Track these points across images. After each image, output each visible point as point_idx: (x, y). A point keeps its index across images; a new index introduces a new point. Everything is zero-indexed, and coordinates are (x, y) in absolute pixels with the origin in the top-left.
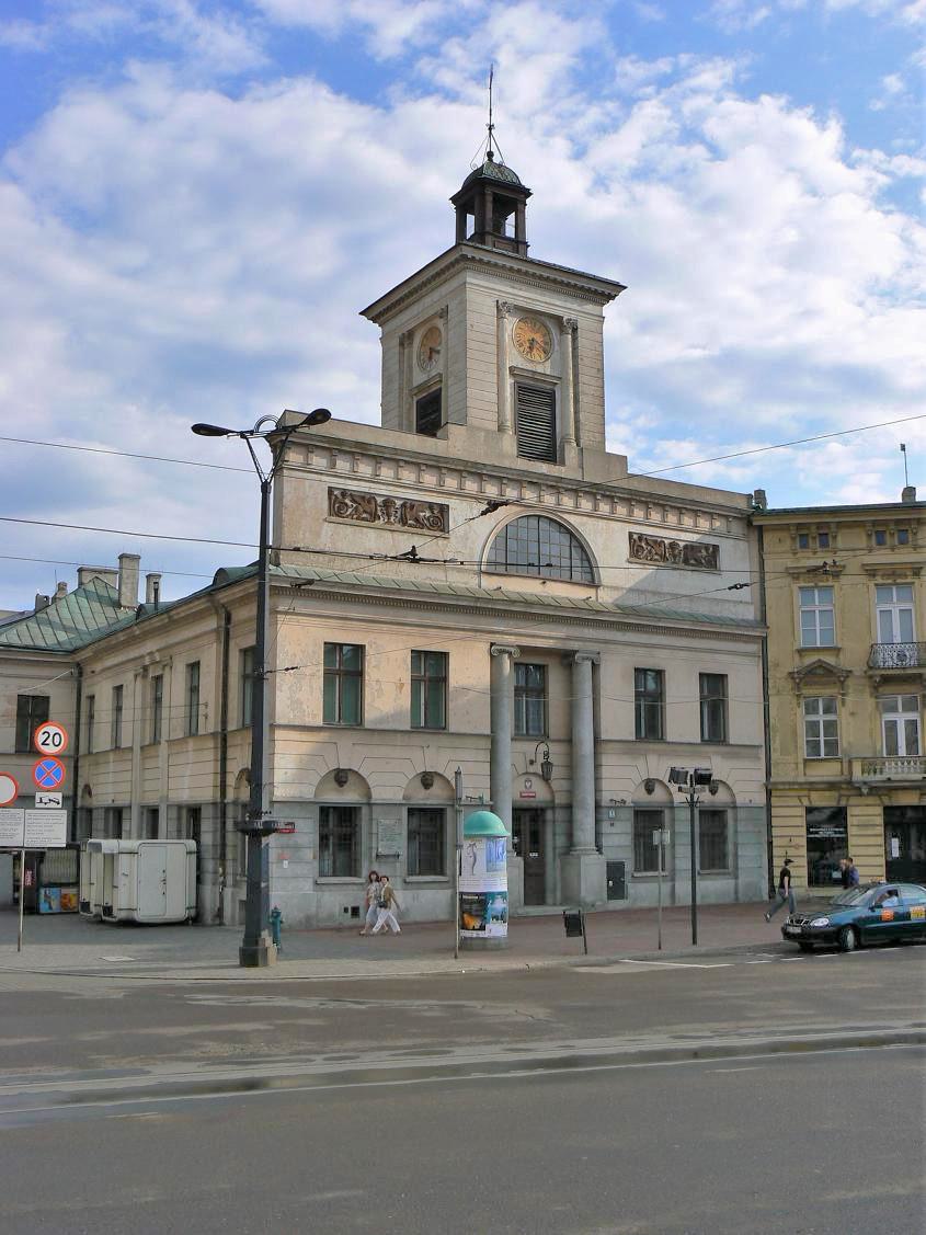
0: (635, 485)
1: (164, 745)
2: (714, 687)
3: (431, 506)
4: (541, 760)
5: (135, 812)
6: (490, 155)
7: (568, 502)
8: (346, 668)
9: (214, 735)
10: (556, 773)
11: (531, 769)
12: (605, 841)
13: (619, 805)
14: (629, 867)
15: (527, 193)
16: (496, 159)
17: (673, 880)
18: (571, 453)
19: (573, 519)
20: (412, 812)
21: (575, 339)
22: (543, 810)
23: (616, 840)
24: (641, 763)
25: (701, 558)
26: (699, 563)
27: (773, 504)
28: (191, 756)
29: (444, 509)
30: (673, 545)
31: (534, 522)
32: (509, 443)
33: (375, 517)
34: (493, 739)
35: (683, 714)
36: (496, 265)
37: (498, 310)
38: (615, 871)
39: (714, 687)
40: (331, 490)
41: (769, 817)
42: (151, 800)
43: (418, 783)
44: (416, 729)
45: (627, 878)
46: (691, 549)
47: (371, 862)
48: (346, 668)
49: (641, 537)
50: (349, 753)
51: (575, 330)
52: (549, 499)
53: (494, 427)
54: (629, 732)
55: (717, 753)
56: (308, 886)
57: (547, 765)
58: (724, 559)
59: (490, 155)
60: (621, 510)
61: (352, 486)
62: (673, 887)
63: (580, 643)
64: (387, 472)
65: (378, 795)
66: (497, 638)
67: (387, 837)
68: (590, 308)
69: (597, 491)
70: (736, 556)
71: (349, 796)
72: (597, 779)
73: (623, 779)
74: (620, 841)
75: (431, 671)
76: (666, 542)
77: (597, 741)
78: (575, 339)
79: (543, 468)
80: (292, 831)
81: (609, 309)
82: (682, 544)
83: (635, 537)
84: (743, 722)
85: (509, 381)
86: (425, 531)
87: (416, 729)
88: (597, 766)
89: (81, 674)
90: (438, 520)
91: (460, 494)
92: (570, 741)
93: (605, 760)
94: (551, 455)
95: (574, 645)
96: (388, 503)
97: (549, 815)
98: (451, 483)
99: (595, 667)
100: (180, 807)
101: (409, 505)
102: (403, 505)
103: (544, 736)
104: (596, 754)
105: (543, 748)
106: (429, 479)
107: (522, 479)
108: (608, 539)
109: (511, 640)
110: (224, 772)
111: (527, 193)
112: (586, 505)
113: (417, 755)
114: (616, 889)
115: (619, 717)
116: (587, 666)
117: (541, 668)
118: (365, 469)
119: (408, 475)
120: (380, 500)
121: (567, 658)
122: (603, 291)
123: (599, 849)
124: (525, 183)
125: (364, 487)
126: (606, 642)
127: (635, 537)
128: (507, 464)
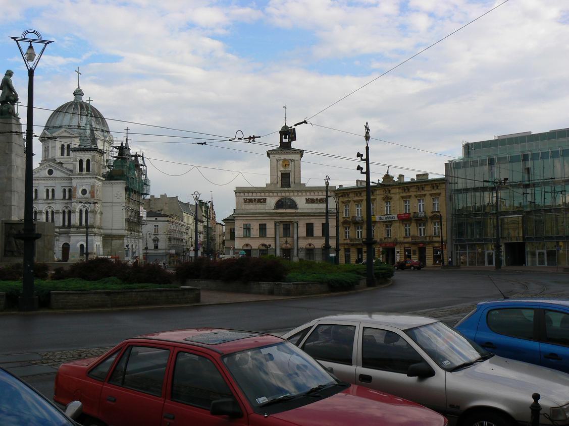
0: (307, 189)
3: (263, 199)
7: (292, 194)
8: (247, 229)
13: (302, 249)
18: (292, 185)
20: (260, 250)
23: (301, 255)
29: (266, 199)
32: (279, 185)
33: (252, 202)
34: (275, 238)
35: (318, 231)
40: (244, 199)
44: (260, 237)
48: (247, 229)
49: (309, 198)
50: (247, 241)
52: (287, 194)
54: (304, 234)
60: (304, 194)
64: (254, 194)
65: (253, 248)
66: (276, 220)
69: (298, 191)
71: (249, 248)
73: (303, 244)
75: (263, 228)
77: (298, 237)
79: (286, 189)
85: (280, 174)
87: (260, 237)
90: (265, 201)
91: (269, 196)
94: (289, 186)
96: (255, 200)
98: (267, 194)
106: (263, 194)
107: (281, 192)
112: (296, 194)
113: (260, 241)
115: (302, 232)
116: (295, 224)
117: (289, 224)
118: (250, 194)
119: (259, 194)
125: (250, 197)
126: (299, 219)
128: (278, 189)
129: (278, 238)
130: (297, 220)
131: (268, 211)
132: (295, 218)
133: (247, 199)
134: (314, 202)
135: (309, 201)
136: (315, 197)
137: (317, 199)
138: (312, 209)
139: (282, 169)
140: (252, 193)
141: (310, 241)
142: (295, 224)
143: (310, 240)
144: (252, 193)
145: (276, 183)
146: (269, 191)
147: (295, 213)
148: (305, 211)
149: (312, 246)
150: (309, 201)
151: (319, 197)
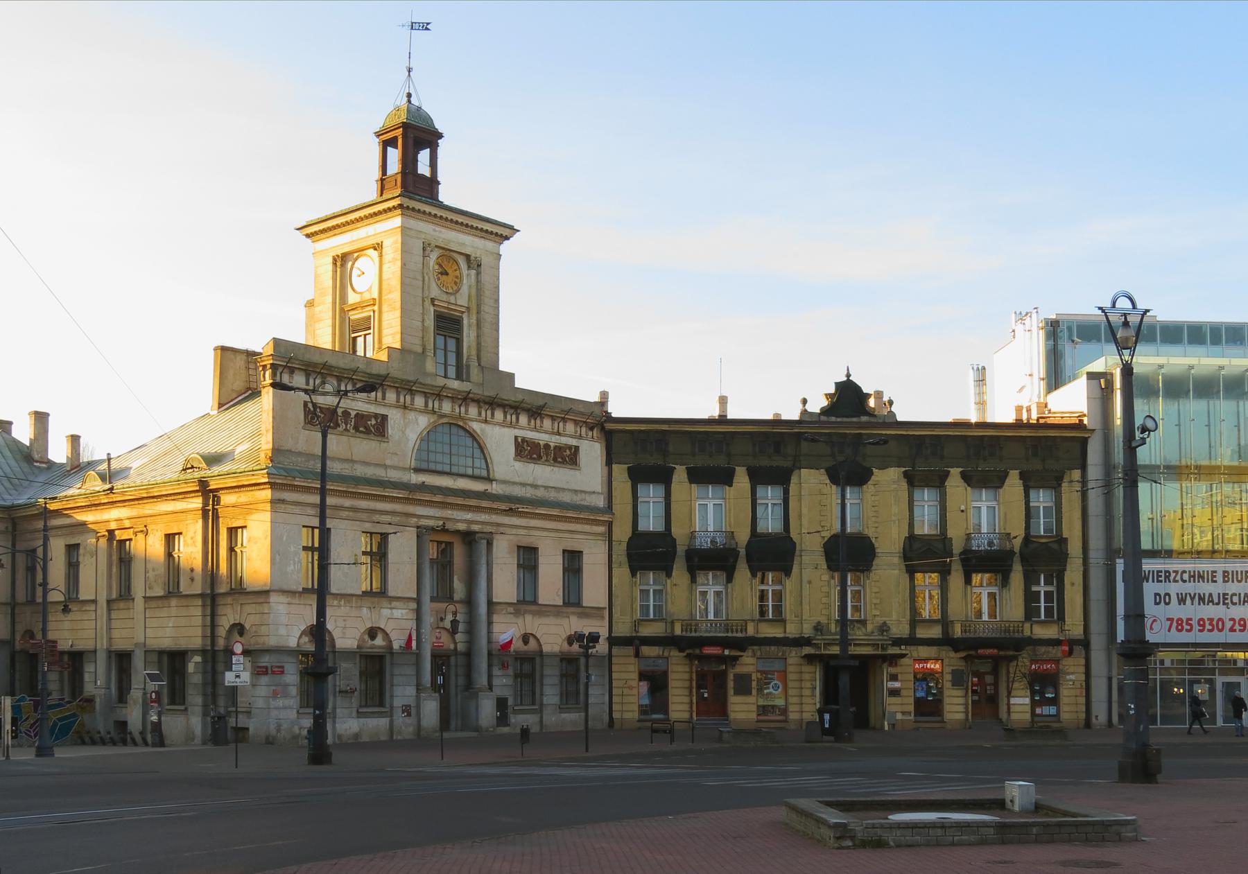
1: (139, 603)
2: (573, 560)
3: (376, 416)
4: (450, 617)
5: (101, 658)
6: (409, 95)
7: (473, 411)
9: (202, 596)
10: (461, 627)
11: (441, 625)
12: (495, 682)
14: (510, 702)
15: (440, 136)
16: (414, 101)
17: (541, 711)
18: (475, 373)
19: (476, 426)
21: (478, 274)
22: (449, 657)
25: (567, 457)
27: (618, 409)
28: (174, 611)
29: (384, 418)
30: (547, 446)
31: (446, 429)
33: (337, 425)
34: (418, 601)
36: (424, 212)
37: (424, 249)
38: (501, 704)
39: (573, 560)
40: (305, 404)
41: (610, 660)
42: (120, 645)
43: (366, 637)
45: (510, 710)
46: (559, 449)
47: (335, 696)
49: (524, 440)
51: (479, 266)
53: (420, 350)
55: (573, 613)
56: (293, 714)
57: (455, 623)
58: (583, 457)
59: (409, 95)
62: (541, 718)
67: (348, 675)
68: (490, 245)
69: (492, 403)
70: (592, 452)
72: (489, 632)
74: (503, 683)
77: (490, 603)
78: (478, 274)
80: (282, 672)
81: (505, 248)
84: (594, 591)
86: (372, 437)
88: (490, 623)
89: (14, 529)
90: (375, 427)
92: (470, 602)
93: (495, 618)
95: (475, 528)
97: (453, 660)
99: (490, 544)
100: (161, 653)
101: (361, 418)
102: (357, 415)
103: (449, 598)
104: (490, 613)
105: (452, 608)
108: (499, 438)
110: (213, 626)
111: (440, 136)
114: (502, 720)
115: (504, 581)
117: (450, 544)
121: (469, 538)
122: (500, 232)
123: (490, 687)
124: (439, 126)
126: (498, 525)
129: (426, 598)
130: (488, 529)
131: (394, 475)
132: (483, 517)
134: (540, 457)
135: (527, 451)
136: (542, 438)
138: (535, 486)
139: (435, 292)
140: (324, 376)
141: (533, 624)
142: (483, 545)
144: (339, 379)
146: (407, 387)
148: (518, 491)
151: (554, 440)
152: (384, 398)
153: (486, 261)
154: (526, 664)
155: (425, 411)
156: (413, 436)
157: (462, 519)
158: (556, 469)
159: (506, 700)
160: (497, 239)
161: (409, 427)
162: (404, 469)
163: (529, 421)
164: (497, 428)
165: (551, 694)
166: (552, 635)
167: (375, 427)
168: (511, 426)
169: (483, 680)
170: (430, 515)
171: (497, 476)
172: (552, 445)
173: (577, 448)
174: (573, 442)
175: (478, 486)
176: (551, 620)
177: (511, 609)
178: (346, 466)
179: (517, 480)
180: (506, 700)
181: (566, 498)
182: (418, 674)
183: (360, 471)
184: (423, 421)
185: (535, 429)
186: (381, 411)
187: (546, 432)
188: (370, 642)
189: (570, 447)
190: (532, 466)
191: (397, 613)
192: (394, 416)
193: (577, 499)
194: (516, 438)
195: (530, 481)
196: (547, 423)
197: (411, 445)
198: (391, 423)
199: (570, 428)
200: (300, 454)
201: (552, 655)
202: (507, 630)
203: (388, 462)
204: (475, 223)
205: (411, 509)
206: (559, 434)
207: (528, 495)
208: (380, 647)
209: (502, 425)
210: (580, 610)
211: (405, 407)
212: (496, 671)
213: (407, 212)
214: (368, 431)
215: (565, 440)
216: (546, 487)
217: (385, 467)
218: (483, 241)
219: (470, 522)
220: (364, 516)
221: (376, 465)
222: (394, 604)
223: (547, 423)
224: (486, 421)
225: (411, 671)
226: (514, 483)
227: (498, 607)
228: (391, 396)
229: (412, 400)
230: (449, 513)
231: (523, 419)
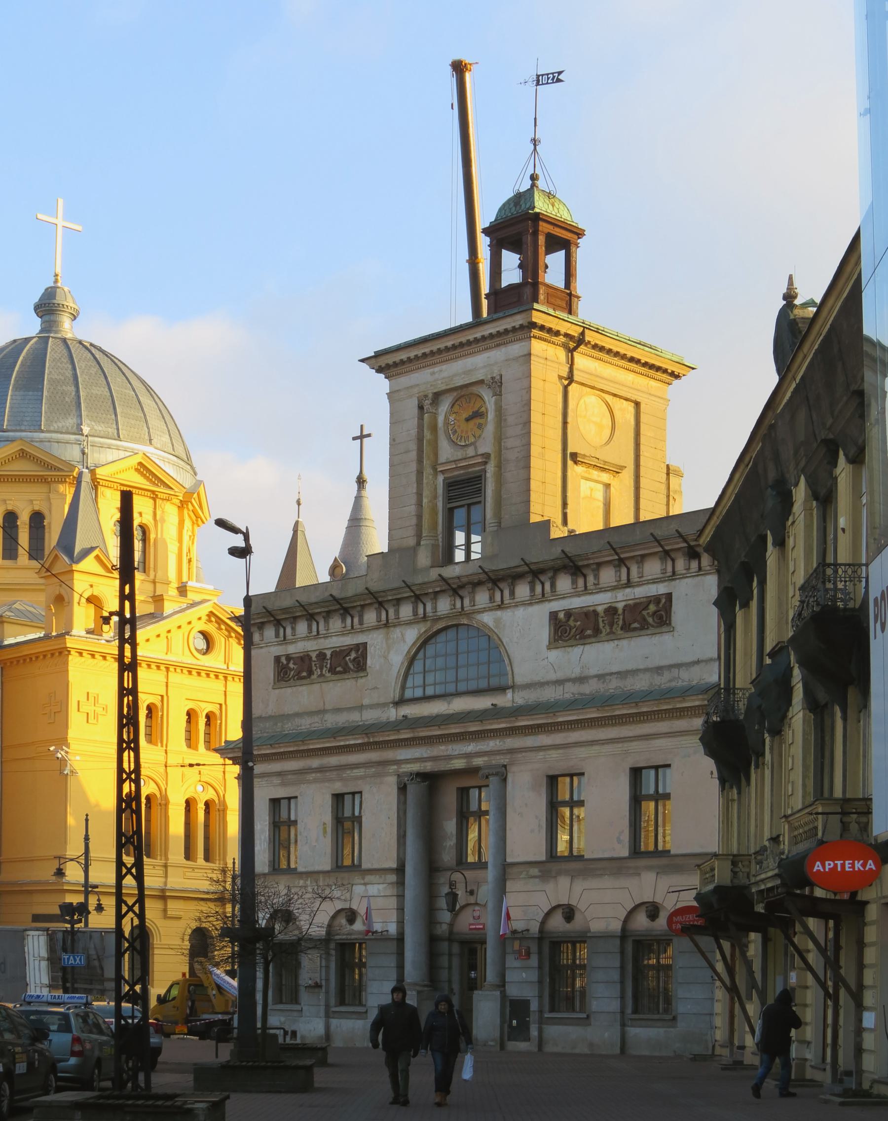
14: (534, 1006)
19: (487, 618)
24: (550, 887)
25: (655, 615)
26: (644, 626)
36: (402, 362)
46: (636, 609)
49: (569, 614)
55: (649, 868)
61: (292, 649)
63: (486, 759)
76: (600, 609)
82: (620, 606)
83: (561, 615)
93: (510, 885)
95: (478, 761)
96: (321, 656)
101: (340, 654)
109: (415, 767)
120: (314, 656)
126: (511, 751)
127: (561, 615)
132: (492, 744)
133: (289, 658)
134: (597, 631)
135: (568, 630)
136: (599, 601)
137: (611, 611)
141: (562, 890)
143: (564, 882)
145: (412, 542)
147: (495, 712)
148: (549, 694)
149: (577, 924)
150: (568, 630)
151: (622, 598)
152: (361, 623)
153: (509, 374)
154: (555, 950)
155: (416, 620)
156: (398, 659)
157: (456, 755)
158: (624, 643)
159: (526, 1003)
160: (519, 335)
161: (390, 650)
162: (384, 705)
163: (574, 582)
164: (520, 612)
165: (604, 995)
166: (603, 905)
167: (351, 662)
168: (543, 598)
169: (491, 975)
170: (415, 758)
171: (519, 680)
172: (620, 606)
173: (669, 596)
174: (661, 589)
175: (483, 703)
176: (607, 882)
177: (535, 871)
178: (316, 719)
179: (553, 677)
180: (526, 1003)
181: (640, 684)
182: (401, 967)
183: (332, 721)
184: (411, 635)
185: (586, 591)
186: (359, 639)
187: (655, 581)
188: (348, 926)
189: (657, 599)
190: (578, 650)
191: (373, 890)
192: (375, 641)
193: (662, 681)
194: (553, 615)
195: (576, 672)
196: (608, 576)
197: (395, 669)
198: (370, 650)
199: (653, 568)
200: (270, 718)
201: (605, 936)
202: (528, 904)
203: (366, 701)
204: (403, 356)
205: (389, 754)
206: (629, 584)
207: (567, 696)
208: (359, 933)
209: (531, 602)
210: (664, 861)
211: (387, 625)
212: (511, 962)
213: (393, 371)
214: (346, 670)
215: (640, 592)
216: (600, 677)
217: (361, 708)
218: (503, 349)
219: (468, 756)
220: (333, 775)
221: (350, 709)
222: (369, 878)
223: (608, 576)
224: (501, 607)
225: (391, 962)
226: (542, 684)
227: (515, 870)
228: (370, 617)
229: (397, 612)
230: (442, 749)
231: (564, 583)
